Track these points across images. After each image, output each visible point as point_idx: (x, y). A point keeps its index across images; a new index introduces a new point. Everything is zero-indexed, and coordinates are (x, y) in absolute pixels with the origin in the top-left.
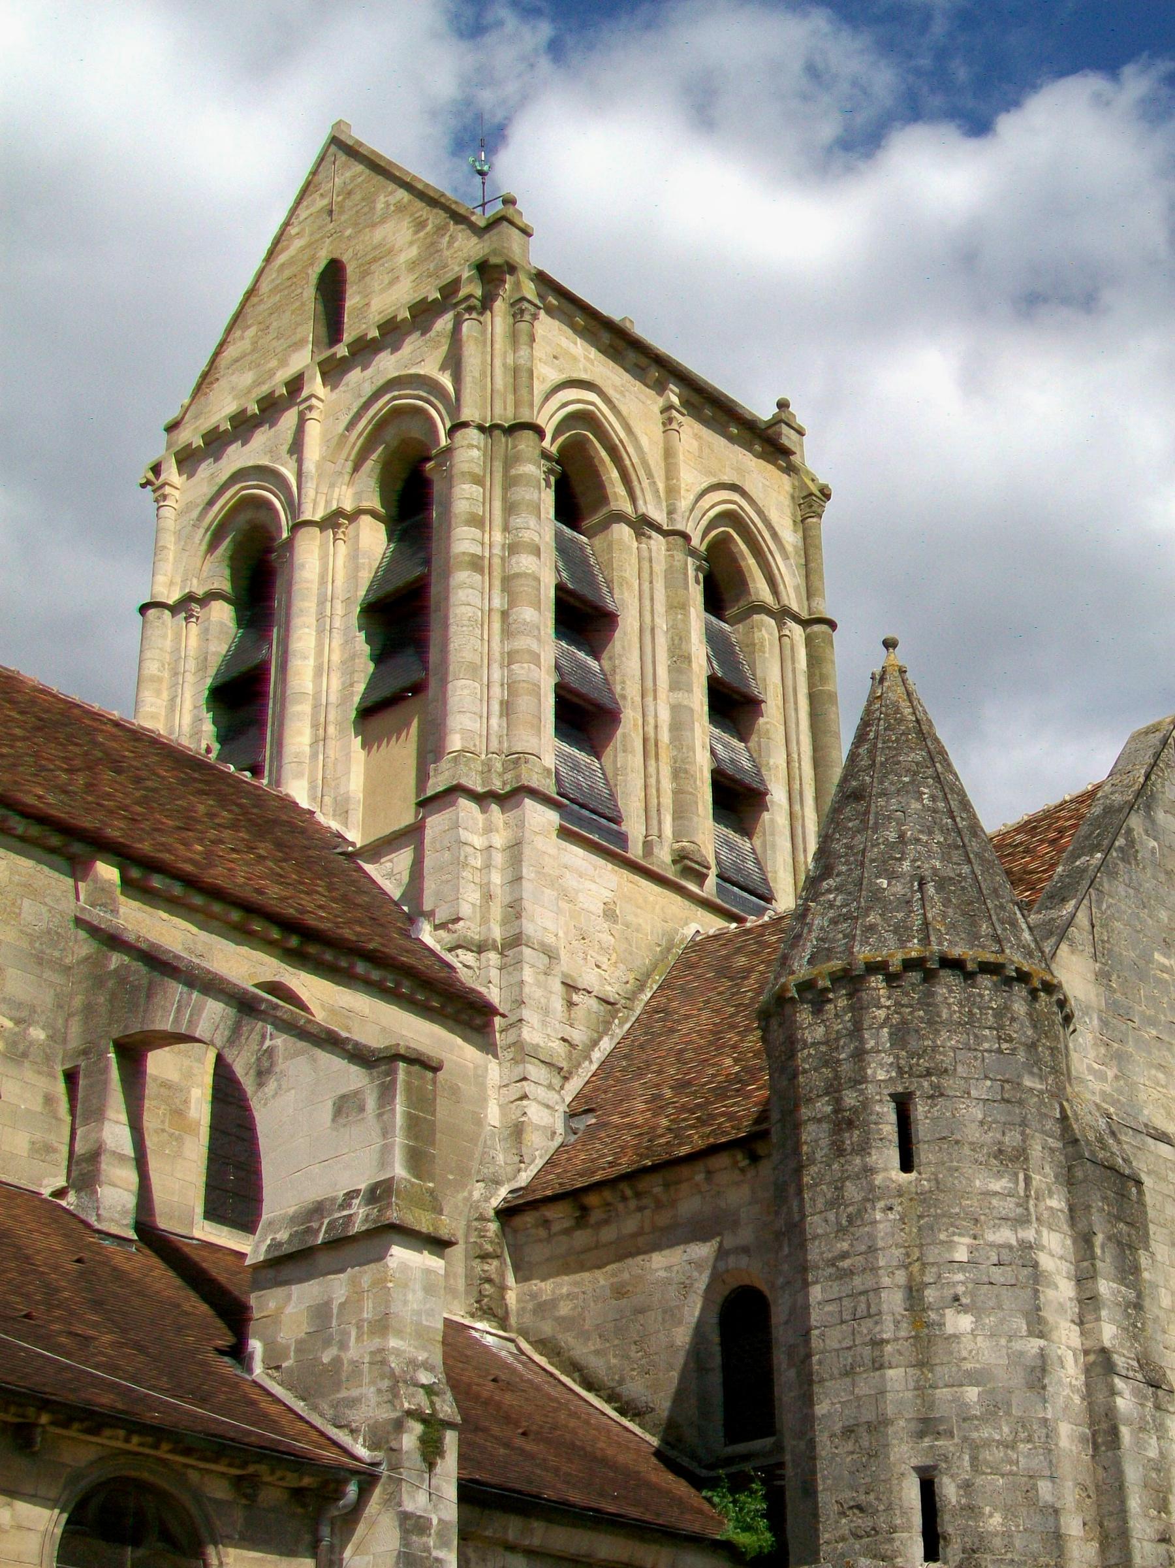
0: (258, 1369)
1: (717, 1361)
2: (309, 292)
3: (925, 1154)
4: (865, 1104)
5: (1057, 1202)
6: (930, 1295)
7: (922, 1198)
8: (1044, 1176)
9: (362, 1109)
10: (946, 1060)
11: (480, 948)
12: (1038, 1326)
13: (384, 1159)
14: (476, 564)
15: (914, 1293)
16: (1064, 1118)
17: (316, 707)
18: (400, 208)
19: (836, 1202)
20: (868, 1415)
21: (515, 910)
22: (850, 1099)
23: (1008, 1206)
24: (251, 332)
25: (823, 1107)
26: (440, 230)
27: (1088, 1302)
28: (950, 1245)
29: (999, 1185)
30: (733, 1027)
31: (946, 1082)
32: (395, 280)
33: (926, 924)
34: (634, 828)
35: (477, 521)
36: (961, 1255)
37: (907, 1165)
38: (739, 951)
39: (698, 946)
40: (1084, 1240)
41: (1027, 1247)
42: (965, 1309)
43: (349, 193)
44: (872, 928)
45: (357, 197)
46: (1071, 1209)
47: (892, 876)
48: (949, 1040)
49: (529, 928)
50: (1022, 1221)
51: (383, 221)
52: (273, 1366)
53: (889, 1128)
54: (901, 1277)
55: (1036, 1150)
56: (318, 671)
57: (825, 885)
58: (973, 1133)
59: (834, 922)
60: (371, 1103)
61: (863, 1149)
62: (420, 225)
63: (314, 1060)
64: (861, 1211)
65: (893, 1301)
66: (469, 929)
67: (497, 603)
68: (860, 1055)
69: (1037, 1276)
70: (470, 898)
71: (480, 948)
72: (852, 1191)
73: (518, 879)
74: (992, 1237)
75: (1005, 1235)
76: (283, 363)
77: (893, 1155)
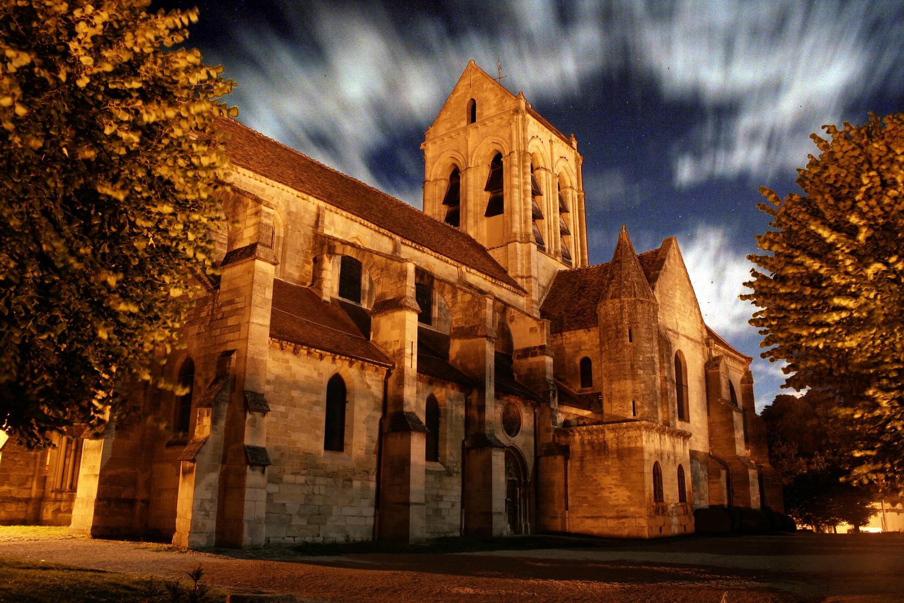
0: (516, 378)
1: (579, 371)
2: (465, 106)
3: (635, 339)
4: (623, 328)
5: (657, 348)
6: (635, 366)
7: (634, 348)
8: (655, 343)
9: (536, 331)
10: (639, 320)
11: (522, 277)
12: (654, 373)
13: (543, 339)
14: (519, 187)
15: (632, 366)
16: (659, 331)
17: (474, 213)
18: (491, 89)
19: (617, 347)
20: (622, 389)
21: (529, 270)
22: (620, 327)
23: (649, 350)
24: (449, 113)
25: (614, 328)
26: (503, 97)
27: (662, 368)
28: (639, 357)
29: (648, 345)
30: (575, 297)
31: (639, 325)
32: (489, 109)
33: (635, 292)
34: (547, 246)
35: (518, 177)
36: (641, 359)
37: (631, 341)
38: (572, 277)
39: (561, 274)
40: (661, 356)
41: (653, 357)
42: (641, 369)
43: (476, 81)
44: (624, 292)
45: (478, 83)
46: (659, 350)
47: (627, 281)
48: (639, 316)
49: (532, 274)
50: (652, 352)
51: (486, 90)
52: (518, 377)
53: (627, 334)
54: (630, 363)
55: (654, 338)
56: (474, 205)
57: (613, 281)
58: (643, 335)
59: (616, 289)
60: (539, 330)
61: (622, 337)
62: (497, 95)
63: (524, 319)
64: (622, 349)
65: (629, 367)
66: (519, 273)
67: (522, 197)
68: (622, 318)
69: (654, 363)
70: (519, 266)
71: (522, 277)
72: (620, 345)
73: (530, 263)
74: (647, 355)
75: (649, 355)
76: (459, 123)
77: (628, 339)
